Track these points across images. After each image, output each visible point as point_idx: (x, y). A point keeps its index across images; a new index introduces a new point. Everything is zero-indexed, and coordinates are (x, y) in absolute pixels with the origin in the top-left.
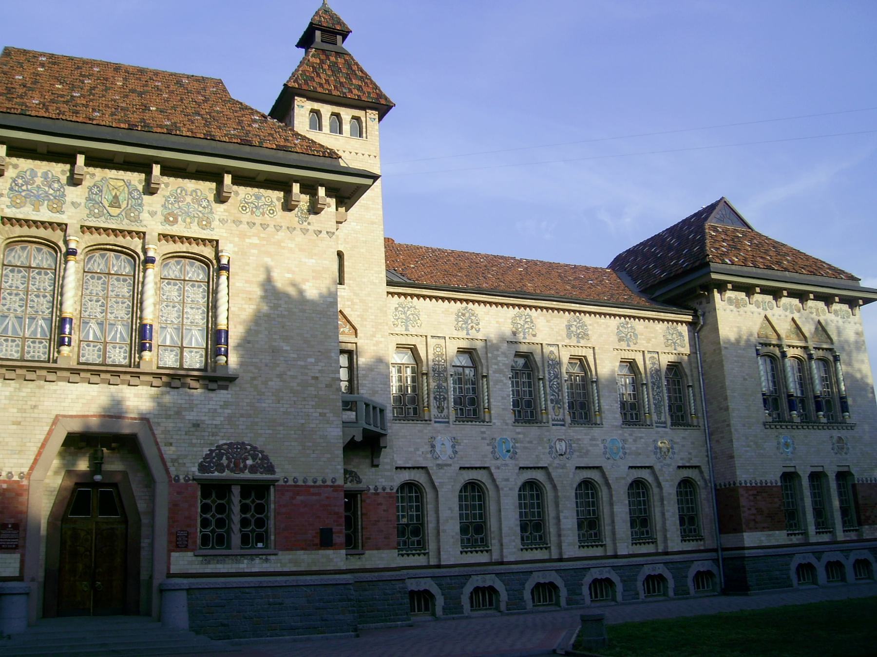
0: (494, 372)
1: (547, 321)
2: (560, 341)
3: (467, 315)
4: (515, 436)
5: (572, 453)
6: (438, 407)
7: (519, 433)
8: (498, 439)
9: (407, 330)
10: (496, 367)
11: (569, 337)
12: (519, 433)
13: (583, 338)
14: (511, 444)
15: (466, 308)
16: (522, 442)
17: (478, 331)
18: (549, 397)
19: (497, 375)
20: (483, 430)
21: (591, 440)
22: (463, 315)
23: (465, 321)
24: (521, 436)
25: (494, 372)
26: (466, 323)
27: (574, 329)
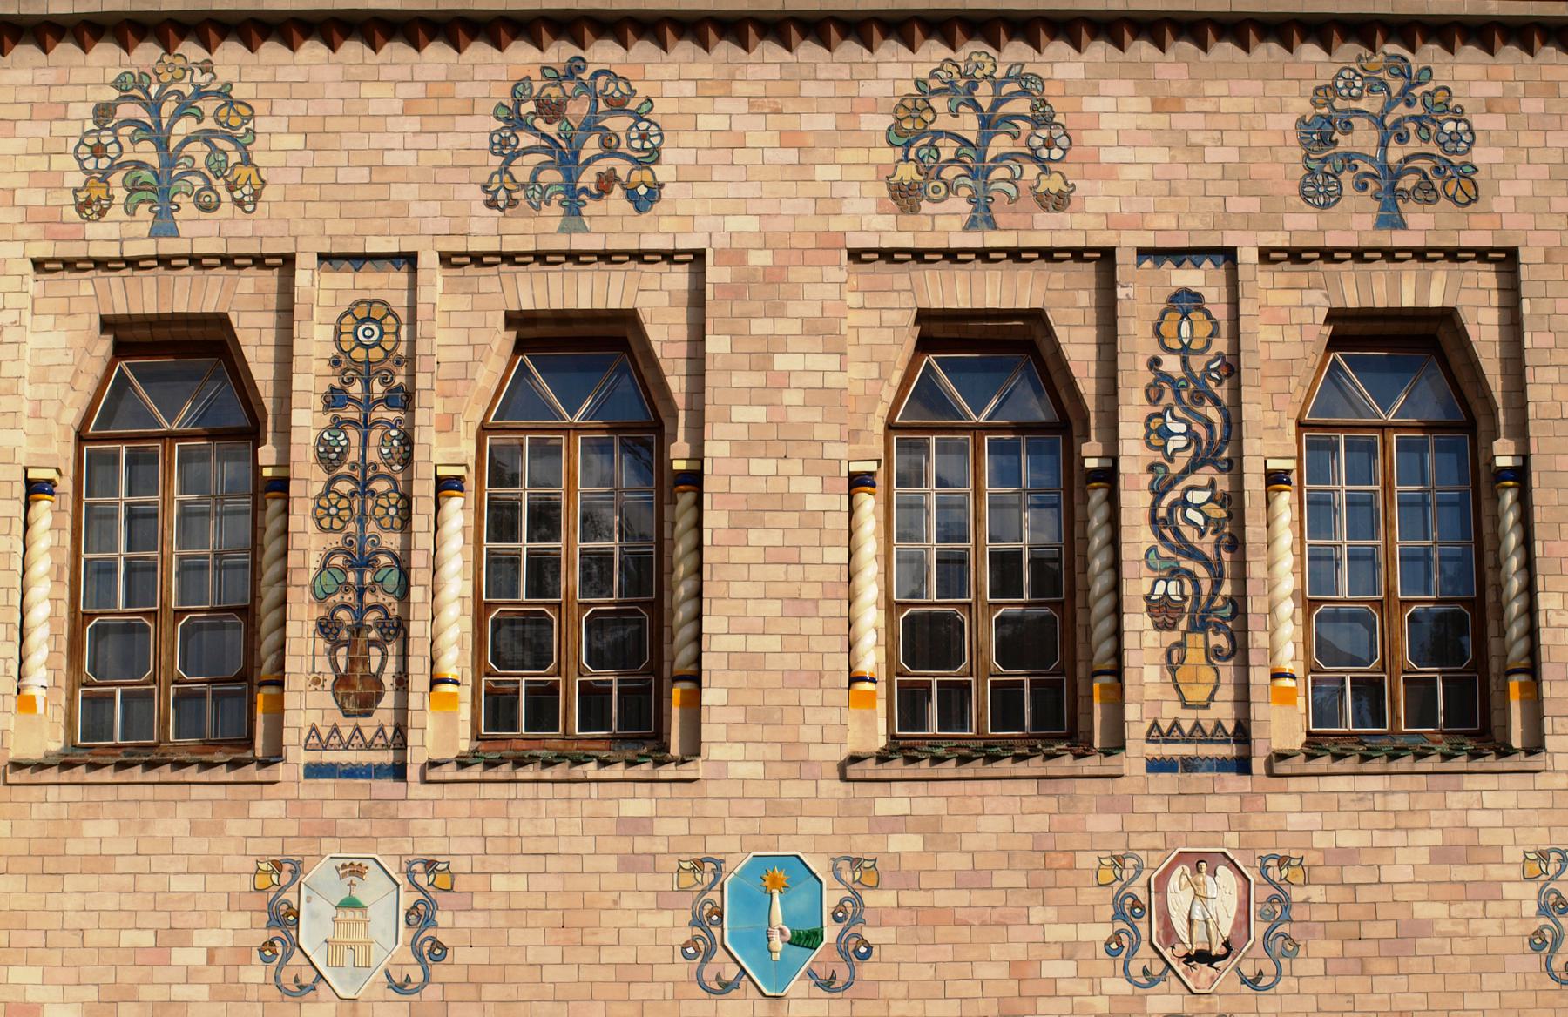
0: (743, 449)
1: (1160, 105)
2: (1250, 222)
3: (578, 109)
4: (862, 845)
5: (1282, 947)
6: (342, 681)
7: (899, 823)
8: (736, 864)
9: (164, 226)
10: (758, 414)
11: (1319, 189)
12: (899, 823)
13: (1426, 193)
14: (830, 900)
15: (574, 69)
16: (910, 881)
17: (645, 199)
18: (1138, 584)
19: (761, 466)
20: (632, 808)
21: (1440, 855)
22: (551, 110)
23: (567, 150)
24: (906, 843)
25: (743, 449)
26: (568, 161)
27: (1362, 139)
